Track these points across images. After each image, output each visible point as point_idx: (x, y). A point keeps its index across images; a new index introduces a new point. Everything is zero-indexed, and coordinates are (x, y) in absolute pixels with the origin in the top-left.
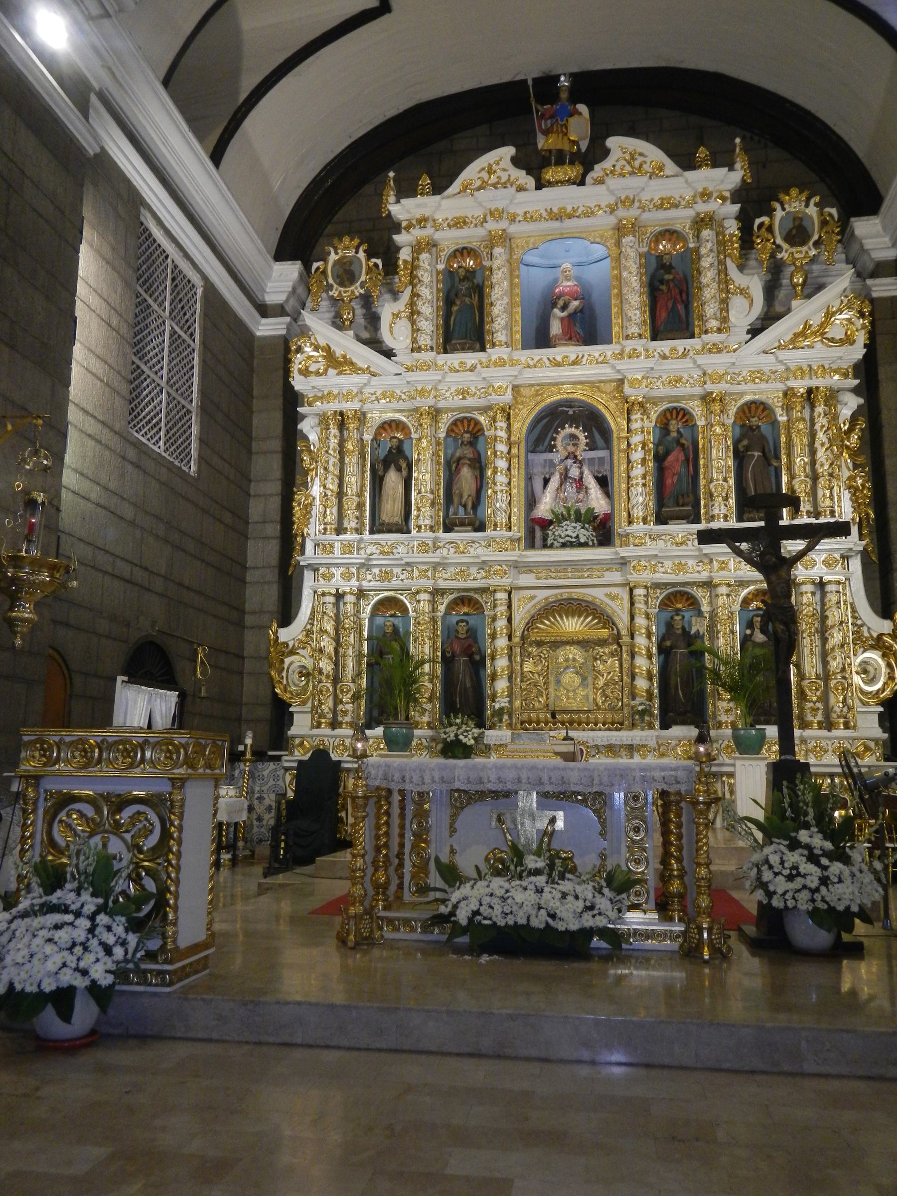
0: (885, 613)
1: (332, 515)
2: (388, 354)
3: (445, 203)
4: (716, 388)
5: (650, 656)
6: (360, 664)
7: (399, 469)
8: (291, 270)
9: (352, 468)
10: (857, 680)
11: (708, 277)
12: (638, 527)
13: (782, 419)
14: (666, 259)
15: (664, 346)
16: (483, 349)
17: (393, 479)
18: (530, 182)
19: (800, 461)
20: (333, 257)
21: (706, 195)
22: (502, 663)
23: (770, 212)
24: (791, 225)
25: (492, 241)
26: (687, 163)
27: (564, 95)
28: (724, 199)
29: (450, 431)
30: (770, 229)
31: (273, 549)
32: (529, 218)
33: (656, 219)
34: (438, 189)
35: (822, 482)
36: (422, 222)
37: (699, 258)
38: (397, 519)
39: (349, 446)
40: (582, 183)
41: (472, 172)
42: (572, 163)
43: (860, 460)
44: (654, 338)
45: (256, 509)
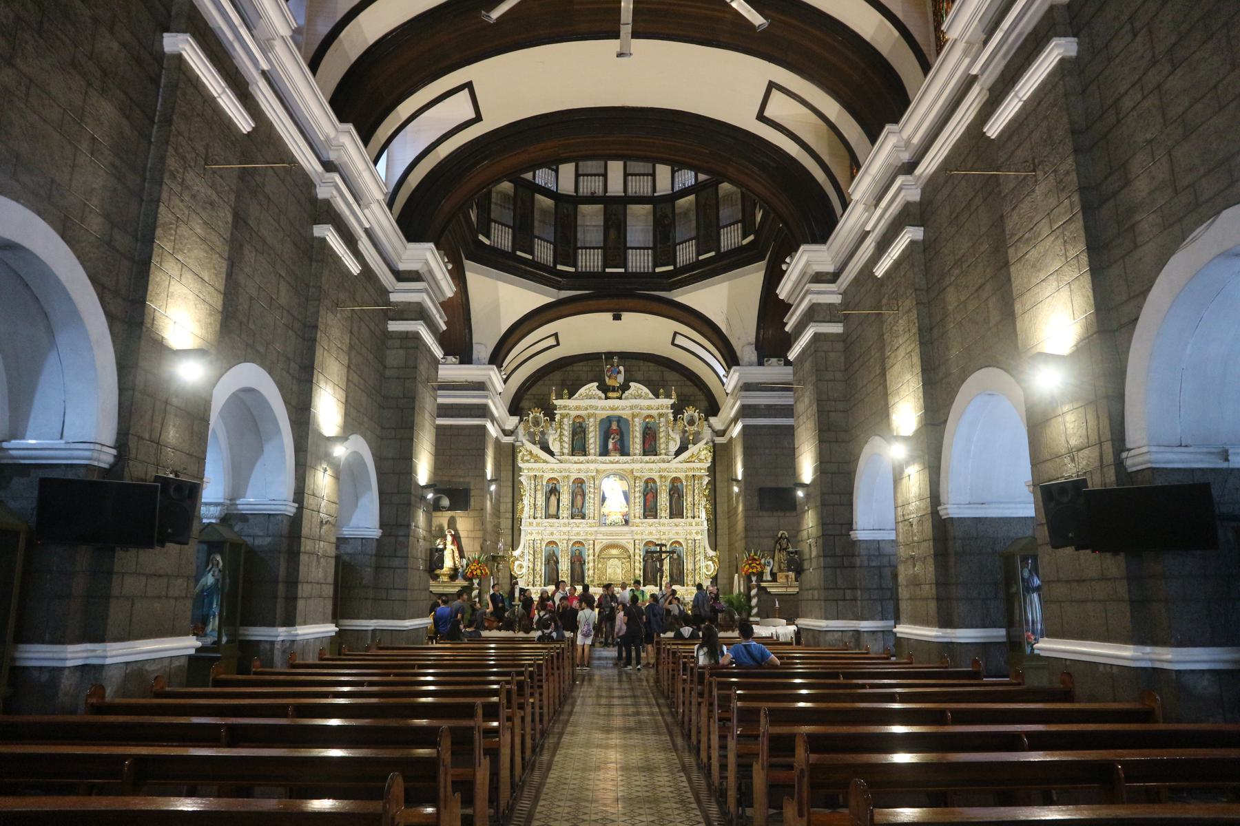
0: (715, 550)
1: (532, 513)
2: (552, 454)
3: (573, 401)
4: (663, 474)
5: (640, 562)
6: (542, 564)
7: (555, 495)
8: (516, 419)
9: (539, 495)
10: (705, 570)
11: (662, 435)
12: (638, 520)
13: (685, 483)
14: (649, 425)
15: (647, 458)
16: (585, 455)
17: (553, 499)
18: (603, 396)
19: (690, 499)
20: (531, 416)
21: (662, 406)
22: (591, 564)
23: (683, 413)
24: (689, 418)
25: (589, 416)
26: (657, 396)
27: (615, 364)
28: (667, 408)
29: (573, 482)
30: (683, 419)
31: (510, 521)
32: (603, 409)
33: (646, 412)
34: (571, 395)
35: (696, 507)
36: (565, 407)
37: (660, 427)
38: (555, 513)
39: (539, 487)
40: (620, 398)
41: (582, 390)
42: (617, 391)
43: (709, 498)
44: (644, 454)
45: (503, 508)
